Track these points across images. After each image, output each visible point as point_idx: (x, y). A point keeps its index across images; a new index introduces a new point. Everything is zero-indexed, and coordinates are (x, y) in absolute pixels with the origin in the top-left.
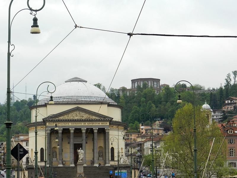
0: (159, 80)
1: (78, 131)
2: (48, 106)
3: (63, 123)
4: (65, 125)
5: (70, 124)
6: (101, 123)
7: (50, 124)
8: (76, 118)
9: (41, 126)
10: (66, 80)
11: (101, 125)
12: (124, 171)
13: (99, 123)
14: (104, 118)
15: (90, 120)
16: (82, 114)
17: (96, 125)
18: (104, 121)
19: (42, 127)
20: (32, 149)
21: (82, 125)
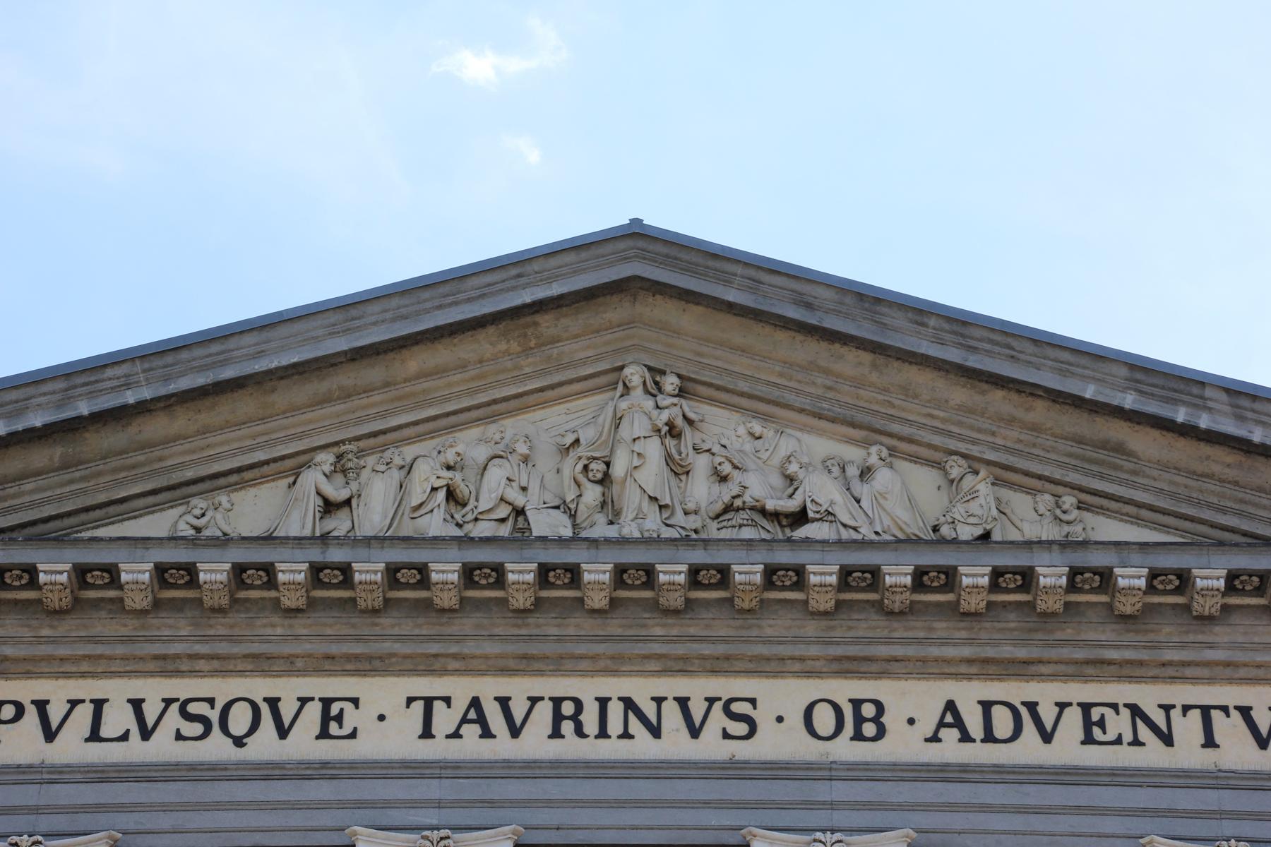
3: (153, 691)
4: (217, 748)
21: (780, 741)
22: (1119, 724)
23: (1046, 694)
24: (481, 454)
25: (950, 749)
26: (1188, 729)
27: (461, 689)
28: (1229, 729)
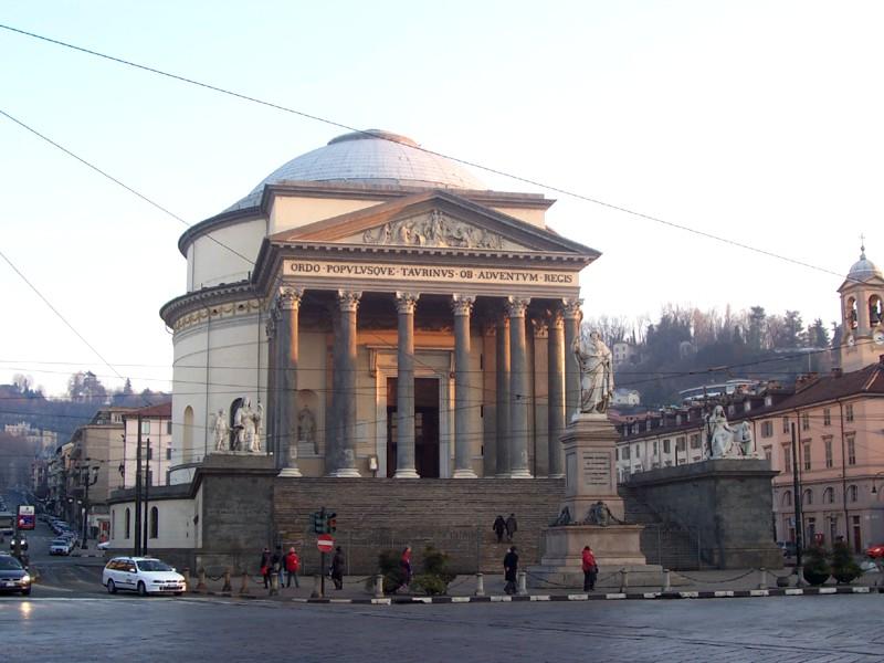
1: (436, 311)
3: (364, 265)
4: (373, 276)
5: (398, 273)
6: (541, 274)
7: (300, 268)
9: (238, 304)
13: (534, 273)
17: (521, 281)
19: (241, 306)
20: (189, 409)
21: (457, 278)
22: (505, 276)
23: (496, 271)
24: (410, 224)
25: (482, 280)
26: (515, 277)
27: (409, 267)
28: (521, 277)
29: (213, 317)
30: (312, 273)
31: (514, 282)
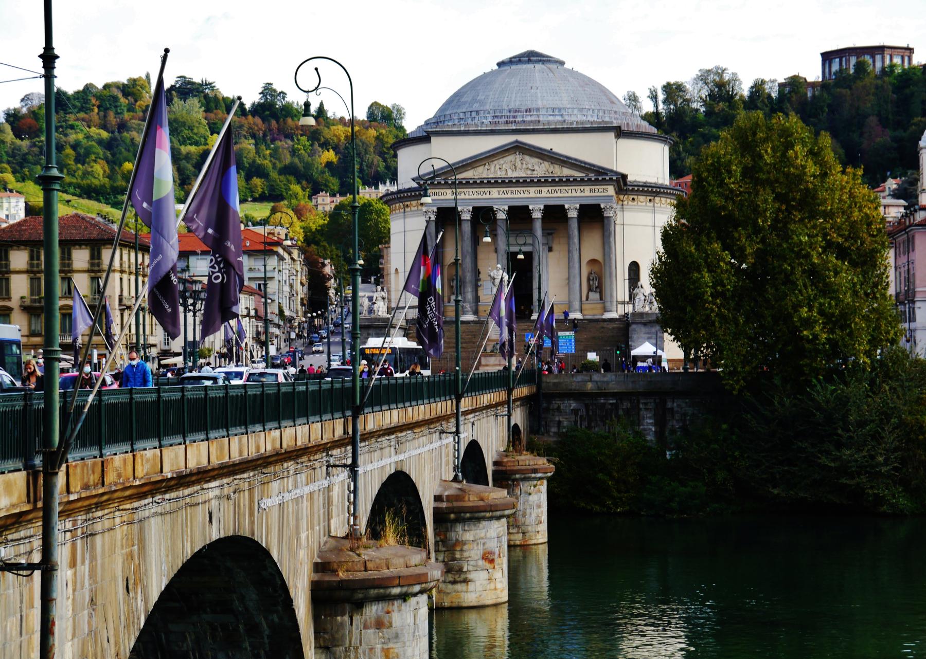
0: (910, 50)
2: (433, 139)
3: (474, 190)
4: (480, 196)
5: (495, 193)
6: (587, 188)
8: (511, 174)
10: (500, 60)
11: (588, 194)
12: (567, 333)
13: (582, 188)
14: (599, 175)
15: (553, 181)
16: (532, 162)
17: (574, 194)
18: (596, 182)
21: (532, 195)
25: (548, 195)
27: (502, 189)
29: (407, 209)
30: (442, 197)
31: (570, 194)
